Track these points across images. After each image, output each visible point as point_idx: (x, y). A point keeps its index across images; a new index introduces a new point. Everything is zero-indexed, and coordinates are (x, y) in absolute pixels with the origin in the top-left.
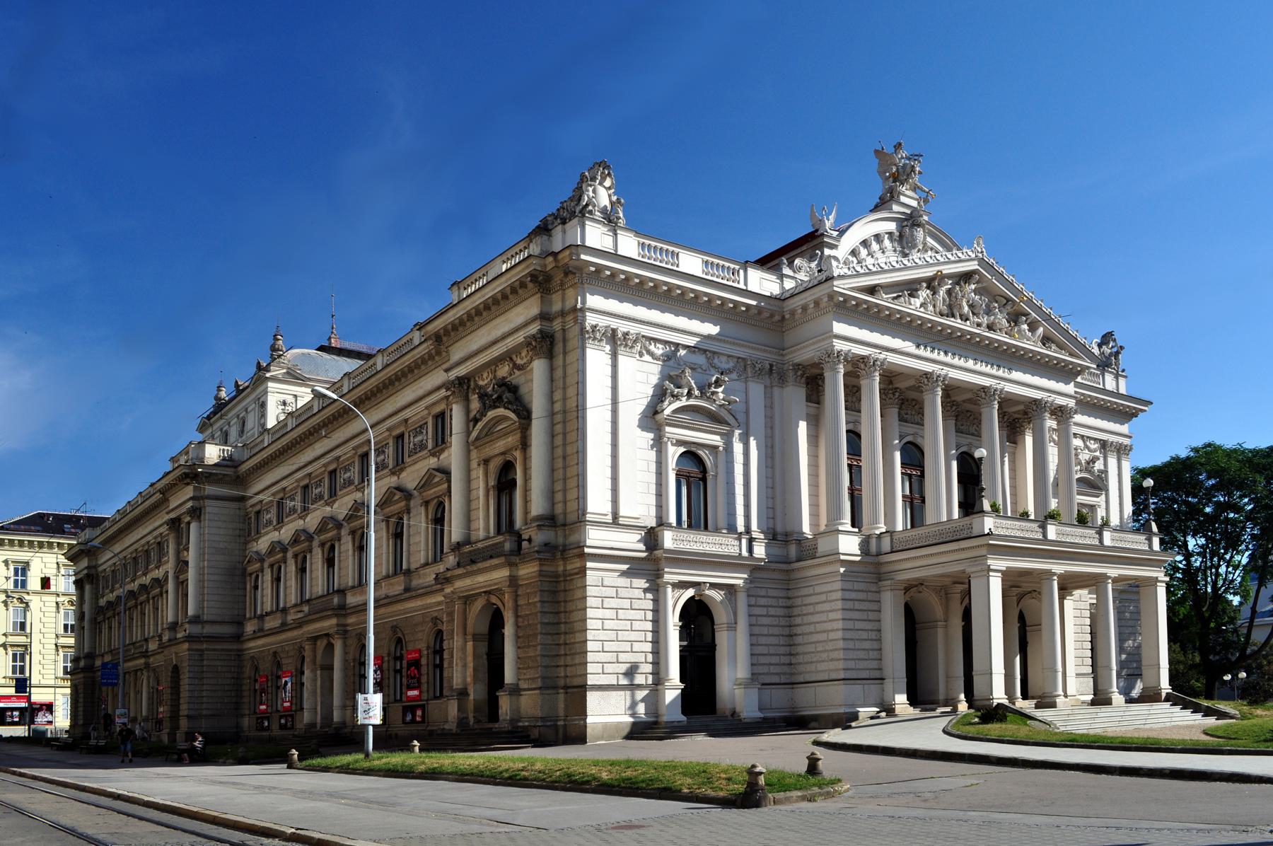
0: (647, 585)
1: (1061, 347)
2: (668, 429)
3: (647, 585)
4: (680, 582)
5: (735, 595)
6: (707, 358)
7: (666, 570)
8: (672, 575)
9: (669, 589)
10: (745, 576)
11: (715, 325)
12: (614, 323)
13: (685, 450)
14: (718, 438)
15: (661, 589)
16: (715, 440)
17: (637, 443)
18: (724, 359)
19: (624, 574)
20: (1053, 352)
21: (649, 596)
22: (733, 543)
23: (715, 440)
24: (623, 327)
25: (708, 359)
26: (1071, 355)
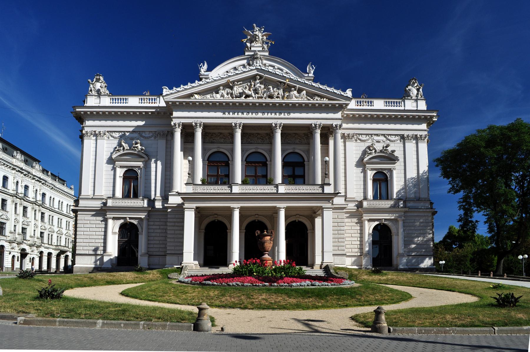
1: (322, 97)
2: (116, 163)
3: (357, 221)
4: (370, 219)
7: (364, 215)
8: (366, 217)
9: (366, 222)
10: (146, 214)
11: (142, 121)
12: (94, 129)
13: (127, 169)
14: (141, 163)
15: (363, 222)
16: (140, 164)
17: (105, 169)
18: (147, 133)
19: (93, 215)
20: (317, 100)
21: (104, 223)
23: (140, 164)
24: (98, 130)
25: (139, 134)
26: (330, 99)
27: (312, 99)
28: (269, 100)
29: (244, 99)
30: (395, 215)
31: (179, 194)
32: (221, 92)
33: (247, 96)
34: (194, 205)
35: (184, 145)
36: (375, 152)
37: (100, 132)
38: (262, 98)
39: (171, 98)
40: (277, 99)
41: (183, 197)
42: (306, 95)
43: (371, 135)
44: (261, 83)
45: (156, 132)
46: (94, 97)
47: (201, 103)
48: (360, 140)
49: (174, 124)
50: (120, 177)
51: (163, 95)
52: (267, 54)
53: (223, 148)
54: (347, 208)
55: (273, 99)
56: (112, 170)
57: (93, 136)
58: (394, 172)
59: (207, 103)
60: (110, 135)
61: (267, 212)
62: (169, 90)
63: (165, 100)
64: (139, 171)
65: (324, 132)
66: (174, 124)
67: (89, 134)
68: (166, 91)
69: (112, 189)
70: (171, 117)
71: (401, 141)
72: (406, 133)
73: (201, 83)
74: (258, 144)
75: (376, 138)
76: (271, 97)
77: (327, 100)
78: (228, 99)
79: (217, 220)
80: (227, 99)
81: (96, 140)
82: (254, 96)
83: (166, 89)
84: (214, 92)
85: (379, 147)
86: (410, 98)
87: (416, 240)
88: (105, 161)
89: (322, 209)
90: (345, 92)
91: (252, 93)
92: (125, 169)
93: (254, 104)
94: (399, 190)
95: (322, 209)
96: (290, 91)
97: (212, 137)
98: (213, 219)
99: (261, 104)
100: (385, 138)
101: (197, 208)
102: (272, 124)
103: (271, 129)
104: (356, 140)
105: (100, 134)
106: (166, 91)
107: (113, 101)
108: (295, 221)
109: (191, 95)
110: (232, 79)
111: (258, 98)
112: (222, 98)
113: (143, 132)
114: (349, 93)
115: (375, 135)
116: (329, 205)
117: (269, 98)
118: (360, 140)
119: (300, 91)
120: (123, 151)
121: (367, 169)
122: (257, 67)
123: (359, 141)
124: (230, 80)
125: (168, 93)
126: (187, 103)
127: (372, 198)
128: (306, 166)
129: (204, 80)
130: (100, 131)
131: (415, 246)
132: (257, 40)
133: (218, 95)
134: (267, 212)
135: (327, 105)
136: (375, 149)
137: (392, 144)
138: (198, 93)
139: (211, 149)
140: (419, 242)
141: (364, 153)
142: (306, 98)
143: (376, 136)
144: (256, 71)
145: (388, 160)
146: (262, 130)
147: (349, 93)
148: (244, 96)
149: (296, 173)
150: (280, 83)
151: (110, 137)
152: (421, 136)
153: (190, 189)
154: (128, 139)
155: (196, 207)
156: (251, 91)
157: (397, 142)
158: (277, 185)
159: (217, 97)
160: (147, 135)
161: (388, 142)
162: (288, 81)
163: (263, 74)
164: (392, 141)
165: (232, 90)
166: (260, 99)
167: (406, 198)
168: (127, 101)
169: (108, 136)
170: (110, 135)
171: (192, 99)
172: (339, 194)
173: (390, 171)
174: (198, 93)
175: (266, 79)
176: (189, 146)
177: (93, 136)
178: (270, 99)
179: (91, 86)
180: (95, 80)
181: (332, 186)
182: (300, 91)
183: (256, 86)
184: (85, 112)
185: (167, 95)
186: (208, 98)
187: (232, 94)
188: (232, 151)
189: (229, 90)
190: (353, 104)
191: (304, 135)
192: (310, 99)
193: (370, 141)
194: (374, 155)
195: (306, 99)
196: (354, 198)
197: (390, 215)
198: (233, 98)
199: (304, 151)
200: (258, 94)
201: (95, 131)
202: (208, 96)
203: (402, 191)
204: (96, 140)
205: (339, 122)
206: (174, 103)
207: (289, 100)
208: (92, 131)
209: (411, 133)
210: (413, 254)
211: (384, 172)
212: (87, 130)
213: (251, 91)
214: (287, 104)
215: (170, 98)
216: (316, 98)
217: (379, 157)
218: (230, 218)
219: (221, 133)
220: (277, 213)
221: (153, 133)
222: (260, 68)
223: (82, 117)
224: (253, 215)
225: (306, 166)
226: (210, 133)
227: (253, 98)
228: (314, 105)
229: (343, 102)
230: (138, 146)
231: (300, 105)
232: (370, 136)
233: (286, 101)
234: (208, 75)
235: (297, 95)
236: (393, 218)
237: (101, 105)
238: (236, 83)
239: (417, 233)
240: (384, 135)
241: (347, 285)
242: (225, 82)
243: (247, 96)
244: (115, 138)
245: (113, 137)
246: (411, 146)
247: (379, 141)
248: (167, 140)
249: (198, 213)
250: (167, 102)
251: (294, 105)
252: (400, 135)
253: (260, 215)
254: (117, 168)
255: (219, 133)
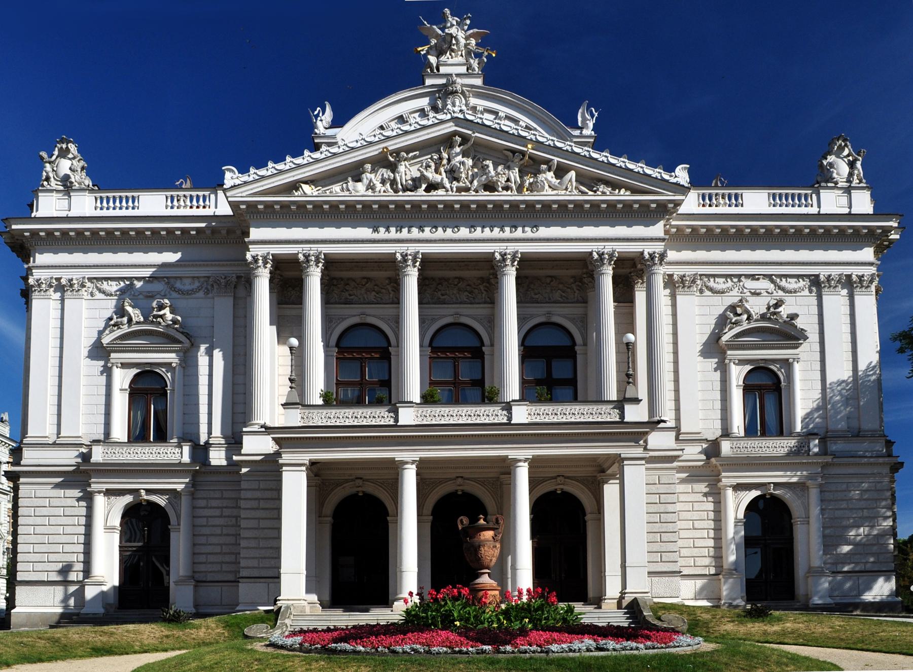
0: (81, 494)
1: (615, 185)
2: (113, 355)
3: (707, 490)
4: (738, 484)
5: (808, 490)
6: (166, 284)
7: (723, 474)
8: (728, 479)
9: (730, 492)
10: (187, 480)
11: (175, 252)
12: (56, 273)
13: (139, 371)
14: (173, 355)
15: (722, 491)
16: (171, 357)
19: (57, 486)
20: (603, 194)
21: (83, 504)
22: (173, 451)
23: (171, 357)
25: (168, 283)
26: (635, 191)
27: (592, 191)
28: (485, 196)
29: (425, 194)
30: (799, 473)
31: (267, 430)
32: (367, 176)
33: (432, 187)
34: (306, 457)
35: (279, 308)
36: (748, 319)
37: (72, 280)
38: (467, 189)
39: (244, 194)
40: (505, 192)
41: (279, 438)
42: (576, 181)
43: (739, 276)
44: (465, 154)
45: (208, 277)
46: (54, 194)
47: (318, 206)
48: (711, 289)
49: (253, 257)
50: (121, 390)
51: (225, 187)
52: (479, 82)
53: (374, 316)
54: (680, 459)
55: (496, 193)
56: (102, 373)
57: (55, 291)
58: (797, 367)
59: (334, 206)
60: (97, 287)
61: (486, 470)
62: (240, 175)
63: (230, 199)
64: (169, 375)
65: (622, 271)
66: (253, 257)
67: (44, 286)
68: (231, 177)
69: (102, 419)
70: (246, 240)
71: (811, 292)
72: (823, 272)
73: (317, 155)
74: (461, 303)
75: (750, 284)
76: (490, 187)
77: (628, 193)
78: (384, 194)
79: (363, 492)
80: (382, 193)
81: (62, 300)
82: (448, 185)
83: (233, 171)
84: (350, 179)
85: (757, 306)
86: (833, 185)
87: (853, 533)
88: (85, 352)
89: (619, 460)
90: (673, 174)
91: (442, 179)
92: (135, 371)
93: (448, 205)
94: (809, 410)
95: (619, 460)
96: (536, 173)
97: (347, 287)
98: (354, 490)
99: (465, 205)
100: (772, 285)
101: (313, 463)
102: (493, 253)
103: (493, 267)
104: (701, 291)
105: (71, 286)
106: (231, 177)
107: (102, 203)
108: (554, 492)
109: (294, 186)
110: (392, 145)
111: (459, 190)
112: (370, 192)
113: (176, 278)
114: (681, 175)
115: (747, 276)
116: (638, 452)
117: (485, 190)
118: (711, 289)
119: (561, 172)
120: (129, 326)
121: (730, 360)
122: (456, 115)
123: (708, 293)
124: (390, 148)
125: (237, 182)
126: (285, 206)
127: (742, 434)
128: (580, 359)
129: (324, 148)
130: (70, 277)
131: (851, 550)
132: (455, 47)
133: (359, 184)
134: (486, 470)
135: (628, 205)
136: (747, 311)
137: (789, 300)
138: (312, 181)
139: (345, 319)
140: (859, 538)
141: (722, 322)
142: (576, 188)
143: (749, 280)
144: (451, 124)
145: (779, 339)
146: (469, 270)
147: (681, 175)
148: (424, 186)
149: (556, 375)
150: (511, 154)
151: (97, 293)
152: (861, 277)
153: (295, 418)
154: (141, 296)
155: (310, 460)
156: (440, 174)
157: (803, 293)
158: (508, 403)
159: (359, 191)
160: (187, 285)
161: (781, 293)
162: (533, 149)
163: (470, 132)
164: (791, 292)
165: (393, 171)
166: (463, 193)
167: (827, 432)
168: (136, 204)
169: (91, 290)
170: (97, 287)
171: (297, 197)
172: (662, 425)
173: (787, 364)
174: (312, 181)
175: (478, 144)
176: (290, 311)
177: (55, 291)
178: (488, 193)
179: (48, 167)
180: (56, 153)
181: (644, 404)
182: (561, 172)
183: (453, 162)
184: (34, 233)
185: (235, 186)
186: (336, 192)
187: (393, 183)
188: (397, 321)
189: (387, 173)
190: (691, 203)
191: (572, 280)
192: (587, 191)
193: (735, 292)
194: (745, 326)
195: (575, 192)
196: (699, 433)
197: (788, 473)
198: (396, 191)
199: (572, 320)
200: (458, 181)
201: (58, 279)
202: (336, 188)
203: (816, 415)
204: (62, 300)
205: (658, 247)
206: (251, 206)
207: (535, 193)
208: (52, 278)
209: (835, 271)
210: (846, 569)
211: (772, 367)
212: (38, 277)
213: (440, 174)
214: (530, 205)
215: (242, 195)
216: (602, 188)
217: (758, 332)
218: (394, 486)
219: (368, 279)
220: (510, 473)
221: (202, 280)
222: (461, 116)
223: (27, 245)
224: (451, 479)
225: (578, 356)
226: (342, 279)
227: (447, 191)
228: (595, 205)
229: (668, 196)
230: (165, 314)
231: (563, 205)
232: (735, 280)
233: (527, 197)
234: (334, 137)
235: (555, 181)
236: (795, 480)
237: (71, 214)
238: (403, 154)
239: (854, 516)
240: (769, 277)
241: (686, 648)
242: (376, 153)
243: (432, 187)
244: (107, 295)
245: (104, 292)
246: (835, 302)
247: (757, 291)
248: (235, 298)
249: (315, 476)
250: (234, 205)
251: (546, 205)
252: (808, 276)
253: (468, 479)
254: (115, 367)
255: (364, 278)
